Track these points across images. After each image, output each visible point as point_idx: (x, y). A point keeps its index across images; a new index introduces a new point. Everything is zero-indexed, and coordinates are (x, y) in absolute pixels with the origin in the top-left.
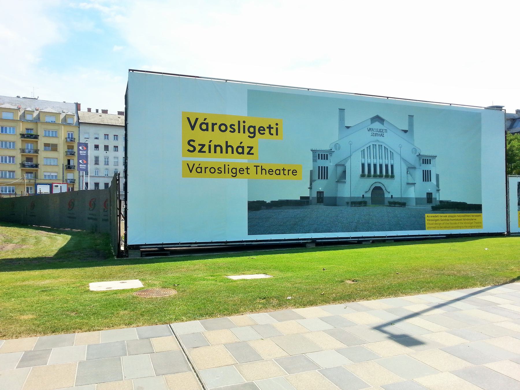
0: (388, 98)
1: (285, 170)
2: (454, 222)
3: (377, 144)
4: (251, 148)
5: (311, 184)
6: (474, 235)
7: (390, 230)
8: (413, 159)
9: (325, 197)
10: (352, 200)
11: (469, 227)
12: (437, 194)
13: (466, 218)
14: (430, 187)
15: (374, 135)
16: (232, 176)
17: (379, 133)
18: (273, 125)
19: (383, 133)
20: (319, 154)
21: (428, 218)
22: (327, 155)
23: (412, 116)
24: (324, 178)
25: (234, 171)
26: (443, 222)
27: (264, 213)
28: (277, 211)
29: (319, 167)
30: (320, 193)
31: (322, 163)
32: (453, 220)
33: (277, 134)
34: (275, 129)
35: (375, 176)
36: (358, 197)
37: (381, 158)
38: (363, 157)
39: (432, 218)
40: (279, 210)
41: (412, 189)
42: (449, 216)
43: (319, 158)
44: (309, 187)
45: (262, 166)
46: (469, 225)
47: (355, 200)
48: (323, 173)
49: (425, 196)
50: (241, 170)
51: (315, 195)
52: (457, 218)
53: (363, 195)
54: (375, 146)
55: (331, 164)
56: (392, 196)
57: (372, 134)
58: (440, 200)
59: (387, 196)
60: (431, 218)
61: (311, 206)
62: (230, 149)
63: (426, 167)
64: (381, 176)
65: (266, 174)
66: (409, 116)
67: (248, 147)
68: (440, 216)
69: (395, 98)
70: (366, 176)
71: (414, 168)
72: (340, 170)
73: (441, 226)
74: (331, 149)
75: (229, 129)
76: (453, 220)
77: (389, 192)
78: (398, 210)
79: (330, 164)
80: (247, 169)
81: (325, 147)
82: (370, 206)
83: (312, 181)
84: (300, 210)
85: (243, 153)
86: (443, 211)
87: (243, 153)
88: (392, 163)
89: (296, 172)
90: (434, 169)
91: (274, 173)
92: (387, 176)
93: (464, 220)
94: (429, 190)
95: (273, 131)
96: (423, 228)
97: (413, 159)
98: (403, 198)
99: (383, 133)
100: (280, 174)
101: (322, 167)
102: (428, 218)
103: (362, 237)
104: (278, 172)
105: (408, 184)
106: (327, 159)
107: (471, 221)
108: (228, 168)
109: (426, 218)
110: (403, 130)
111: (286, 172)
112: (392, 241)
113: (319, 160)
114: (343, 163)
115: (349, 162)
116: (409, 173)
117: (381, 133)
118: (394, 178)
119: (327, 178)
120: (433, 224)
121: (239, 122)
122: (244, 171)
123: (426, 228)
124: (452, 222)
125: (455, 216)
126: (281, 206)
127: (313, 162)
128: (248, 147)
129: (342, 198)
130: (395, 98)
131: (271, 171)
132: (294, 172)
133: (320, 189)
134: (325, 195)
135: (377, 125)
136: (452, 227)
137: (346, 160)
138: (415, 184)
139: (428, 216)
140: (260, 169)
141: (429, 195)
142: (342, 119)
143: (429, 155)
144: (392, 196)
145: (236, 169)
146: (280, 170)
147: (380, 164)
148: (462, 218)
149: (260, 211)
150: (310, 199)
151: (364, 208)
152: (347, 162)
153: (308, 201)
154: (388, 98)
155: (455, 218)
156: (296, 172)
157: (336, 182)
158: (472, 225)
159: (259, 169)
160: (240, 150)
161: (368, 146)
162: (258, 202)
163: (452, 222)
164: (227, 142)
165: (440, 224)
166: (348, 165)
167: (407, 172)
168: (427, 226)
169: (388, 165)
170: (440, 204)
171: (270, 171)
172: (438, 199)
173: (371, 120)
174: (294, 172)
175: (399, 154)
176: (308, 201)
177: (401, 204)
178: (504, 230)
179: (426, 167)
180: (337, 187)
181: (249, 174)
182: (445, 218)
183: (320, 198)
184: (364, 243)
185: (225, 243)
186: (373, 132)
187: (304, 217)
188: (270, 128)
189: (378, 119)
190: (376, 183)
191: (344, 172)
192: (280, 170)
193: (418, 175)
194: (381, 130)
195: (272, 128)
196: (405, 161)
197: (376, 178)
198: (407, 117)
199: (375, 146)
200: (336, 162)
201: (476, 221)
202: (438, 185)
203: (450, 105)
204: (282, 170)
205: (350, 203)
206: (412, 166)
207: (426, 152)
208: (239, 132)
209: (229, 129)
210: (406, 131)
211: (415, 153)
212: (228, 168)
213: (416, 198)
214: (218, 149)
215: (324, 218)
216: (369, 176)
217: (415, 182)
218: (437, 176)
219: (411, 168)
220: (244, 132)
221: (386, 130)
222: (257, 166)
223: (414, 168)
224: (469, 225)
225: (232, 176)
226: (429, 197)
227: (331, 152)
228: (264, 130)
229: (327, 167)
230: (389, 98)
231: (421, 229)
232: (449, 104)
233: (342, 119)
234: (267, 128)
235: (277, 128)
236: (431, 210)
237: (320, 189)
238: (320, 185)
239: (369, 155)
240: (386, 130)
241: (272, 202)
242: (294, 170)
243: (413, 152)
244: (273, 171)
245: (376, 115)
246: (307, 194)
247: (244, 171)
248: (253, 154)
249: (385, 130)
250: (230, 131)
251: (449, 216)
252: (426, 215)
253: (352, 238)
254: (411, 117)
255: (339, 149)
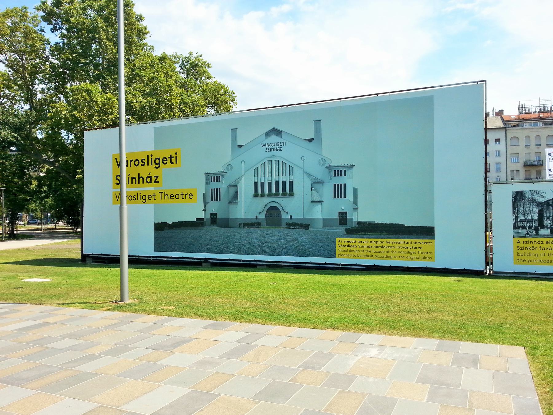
0: (377, 94)
1: (183, 194)
2: (380, 249)
3: (273, 159)
4: (157, 177)
5: (205, 207)
6: (414, 269)
7: (288, 254)
8: (320, 172)
9: (221, 219)
10: (244, 222)
11: (408, 258)
12: (355, 214)
13: (403, 245)
14: (343, 205)
15: (269, 150)
16: (143, 202)
17: (275, 147)
18: (174, 155)
19: (281, 146)
20: (211, 177)
21: (340, 243)
22: (219, 177)
23: (319, 120)
24: (217, 200)
25: (144, 198)
26: (362, 249)
27: (167, 233)
28: (177, 231)
29: (212, 189)
30: (213, 215)
31: (215, 185)
32: (377, 247)
33: (176, 163)
34: (175, 158)
35: (270, 195)
36: (251, 219)
37: (284, 174)
38: (257, 175)
39: (347, 244)
40: (179, 231)
41: (318, 207)
42: (371, 242)
43: (211, 181)
44: (203, 209)
45: (165, 192)
46: (409, 255)
47: (247, 222)
48: (216, 195)
49: (336, 216)
50: (150, 196)
51: (209, 217)
52: (384, 245)
53: (256, 216)
54: (270, 162)
55: (224, 186)
56: (291, 216)
57: (267, 149)
58: (359, 220)
59: (284, 216)
60: (343, 244)
61: (205, 228)
62: (141, 180)
63: (339, 180)
64: (277, 194)
65: (168, 199)
66: (314, 121)
67: (155, 177)
68: (357, 241)
69: (388, 93)
70: (260, 195)
71: (322, 182)
72: (232, 190)
73: (359, 253)
74: (224, 171)
75: (141, 163)
76: (377, 247)
77: (287, 213)
78: (298, 233)
79: (222, 186)
80: (154, 195)
81: (216, 169)
82: (264, 228)
83: (205, 203)
84: (196, 231)
85: (151, 182)
86: (362, 234)
87: (151, 182)
88: (291, 178)
89: (192, 196)
90: (349, 181)
91: (174, 197)
92: (284, 194)
93: (399, 247)
94: (343, 209)
95: (174, 160)
96: (334, 256)
97: (320, 172)
98: (306, 218)
99: (281, 146)
100: (179, 198)
101: (214, 189)
102: (340, 243)
103: (255, 261)
104: (177, 197)
105: (313, 202)
106: (219, 181)
107: (412, 250)
108: (140, 196)
109: (338, 243)
110: (307, 140)
111: (184, 196)
112: (291, 267)
113: (211, 182)
114: (235, 184)
115: (241, 182)
116: (315, 190)
117: (278, 147)
118: (293, 196)
119: (220, 200)
120: (347, 251)
121: (148, 156)
122: (151, 197)
123: (337, 255)
124: (375, 249)
125: (381, 242)
126: (181, 227)
127: (206, 185)
128: (155, 177)
129: (235, 220)
130: (388, 93)
131: (150, 196)
132: (191, 196)
133: (214, 210)
134: (218, 217)
135: (274, 139)
136: (376, 257)
137: (238, 180)
138: (323, 201)
139: (339, 241)
140: (164, 195)
141: (343, 215)
142: (234, 138)
143: (343, 165)
144: (291, 216)
145: (146, 196)
146: (179, 195)
147: (255, 182)
148: (395, 245)
149: (164, 231)
150: (204, 221)
151: (258, 230)
152: (239, 182)
153: (203, 222)
154: (377, 95)
155: (381, 245)
156: (192, 196)
157: (229, 203)
158: (413, 255)
159: (163, 194)
160: (149, 180)
161: (262, 162)
162: (162, 223)
163: (375, 249)
164: (139, 174)
165: (357, 251)
166: (240, 185)
167: (312, 188)
168: (338, 253)
169: (285, 182)
170: (358, 226)
171: (172, 196)
172: (355, 220)
173: (266, 135)
174: (191, 196)
175: (301, 168)
176: (203, 222)
177: (304, 225)
178: (479, 265)
179: (339, 180)
180: (229, 207)
181: (155, 199)
182: (365, 244)
183: (214, 220)
184: (258, 267)
185: (152, 257)
186: (268, 147)
187: (200, 237)
188: (171, 157)
189: (276, 132)
190: (271, 202)
191: (237, 192)
192: (179, 195)
193: (328, 191)
194: (278, 144)
195: (173, 157)
196: (308, 174)
197: (285, 197)
198: (312, 124)
199: (270, 162)
200: (229, 183)
201: (422, 251)
202: (355, 202)
203: (476, 83)
204: (181, 194)
205: (242, 225)
206: (319, 181)
207: (338, 161)
208: (148, 165)
209: (141, 163)
210: (310, 140)
211: (323, 165)
212: (140, 196)
213: (323, 219)
214: (134, 180)
215: (217, 239)
216: (263, 195)
217: (323, 199)
218: (355, 191)
219: (317, 183)
220: (152, 164)
221: (284, 143)
222: (161, 193)
223: (322, 182)
224: (409, 255)
225: (143, 202)
226: (343, 218)
227: (223, 173)
228: (167, 160)
229: (220, 189)
230: (379, 95)
231: (329, 256)
232: (375, 94)
233: (234, 138)
234: (169, 158)
235: (176, 157)
236: (345, 233)
237: (214, 211)
238: (214, 207)
239: (263, 173)
240: (284, 143)
241: (173, 223)
242: (149, 195)
243: (320, 164)
244: (173, 196)
245: (272, 128)
246: (202, 216)
247: (151, 197)
248: (158, 182)
249: (283, 142)
250: (142, 165)
251: (371, 242)
252: (337, 239)
253: (244, 261)
254: (318, 122)
255: (231, 169)
